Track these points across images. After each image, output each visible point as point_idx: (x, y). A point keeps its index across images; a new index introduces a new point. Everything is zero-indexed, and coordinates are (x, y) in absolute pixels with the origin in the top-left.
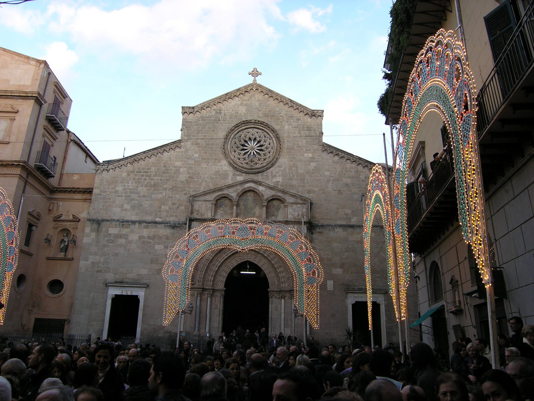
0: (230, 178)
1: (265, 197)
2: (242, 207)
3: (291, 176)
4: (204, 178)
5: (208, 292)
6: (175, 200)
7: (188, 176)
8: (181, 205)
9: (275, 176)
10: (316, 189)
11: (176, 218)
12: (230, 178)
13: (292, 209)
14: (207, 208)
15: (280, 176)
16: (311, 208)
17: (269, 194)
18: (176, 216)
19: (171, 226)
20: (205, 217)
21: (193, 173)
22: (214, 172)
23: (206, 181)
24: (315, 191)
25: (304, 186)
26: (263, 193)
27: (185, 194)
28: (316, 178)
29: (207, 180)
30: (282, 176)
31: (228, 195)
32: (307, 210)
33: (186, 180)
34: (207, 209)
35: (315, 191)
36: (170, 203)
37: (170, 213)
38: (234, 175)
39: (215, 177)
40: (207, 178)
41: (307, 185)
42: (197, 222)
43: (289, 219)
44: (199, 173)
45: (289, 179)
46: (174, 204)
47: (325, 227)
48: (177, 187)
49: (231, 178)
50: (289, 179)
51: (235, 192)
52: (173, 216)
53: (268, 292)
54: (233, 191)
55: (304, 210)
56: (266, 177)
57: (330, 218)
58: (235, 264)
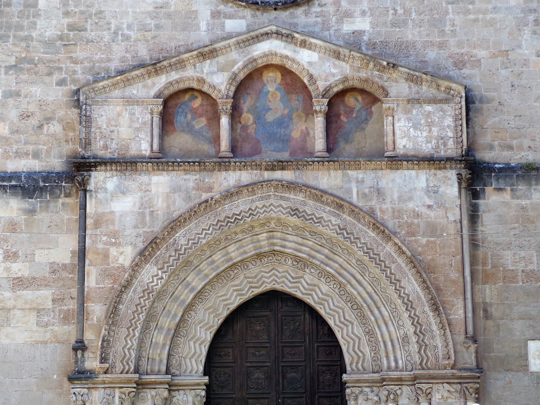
0: (203, 26)
1: (322, 85)
2: (248, 118)
3: (400, 11)
4: (118, 28)
5: (153, 392)
6: (28, 103)
7: (66, 21)
8: (48, 120)
9: (348, 15)
10: (482, 53)
11: (37, 162)
12: (203, 26)
13: (409, 119)
14: (137, 125)
15: (363, 13)
16: (467, 114)
17: (333, 75)
18: (36, 155)
19: (23, 188)
20: (133, 151)
21: (82, 13)
22: (151, 8)
23: (127, 38)
24: (479, 61)
25: (442, 46)
26: (312, 71)
27: (61, 83)
28: (481, 16)
29: (131, 33)
30: (372, 15)
31: (201, 81)
32: (456, 120)
33: (61, 38)
34: (138, 130)
35: (479, 61)
36: (13, 114)
37: (15, 147)
38: (216, 14)
39: (153, 23)
40: (129, 27)
41: (452, 41)
42: (106, 170)
43: (400, 151)
44: (101, 12)
45: (394, 24)
46: (25, 116)
47: (514, 172)
48: (31, 61)
49: (208, 24)
50: (394, 24)
51: (222, 70)
52: (27, 154)
53: (343, 385)
54: (216, 69)
55: (449, 121)
56: (319, 19)
57: (531, 144)
58: (235, 302)
